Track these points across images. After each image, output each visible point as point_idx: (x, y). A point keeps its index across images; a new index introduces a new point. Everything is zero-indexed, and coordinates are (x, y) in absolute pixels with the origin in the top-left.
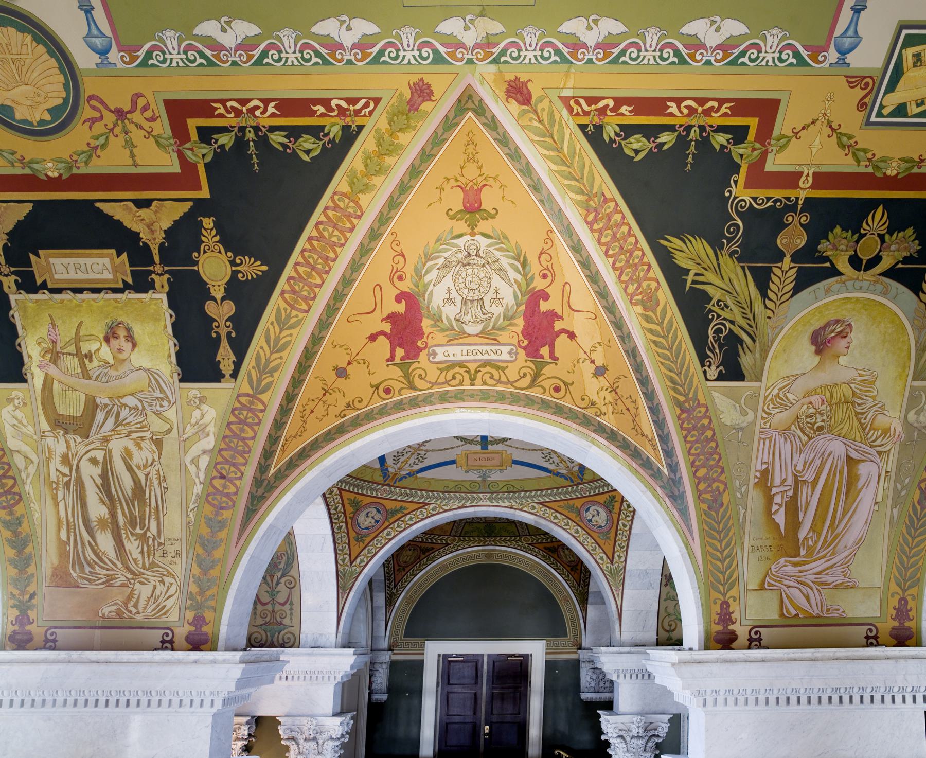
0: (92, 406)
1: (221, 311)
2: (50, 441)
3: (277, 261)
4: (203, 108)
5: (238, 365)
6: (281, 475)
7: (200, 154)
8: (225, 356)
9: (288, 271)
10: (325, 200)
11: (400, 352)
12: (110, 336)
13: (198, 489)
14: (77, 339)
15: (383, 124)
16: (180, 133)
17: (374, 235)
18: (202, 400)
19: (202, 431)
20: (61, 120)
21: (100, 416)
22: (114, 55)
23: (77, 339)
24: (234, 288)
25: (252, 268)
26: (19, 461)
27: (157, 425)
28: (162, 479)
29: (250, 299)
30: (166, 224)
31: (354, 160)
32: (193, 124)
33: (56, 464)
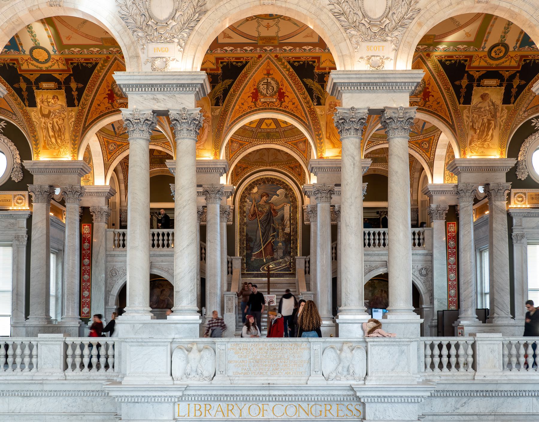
0: (50, 112)
1: (75, 93)
2: (41, 119)
3: (85, 84)
4: (72, 60)
5: (79, 104)
6: (88, 126)
7: (71, 67)
8: (76, 102)
9: (87, 86)
10: (93, 74)
11: (110, 101)
12: (53, 98)
13: (72, 129)
14: (47, 99)
15: (102, 62)
16: (67, 63)
17: (103, 80)
18: (72, 111)
19: (72, 117)
20: (47, 61)
21: (51, 114)
22: (57, 52)
23: (47, 99)
24: (77, 89)
25: (81, 85)
26: (35, 123)
27: (63, 116)
28: (64, 127)
29: (80, 91)
30: (64, 78)
31: (98, 67)
32: (69, 62)
33: (43, 124)
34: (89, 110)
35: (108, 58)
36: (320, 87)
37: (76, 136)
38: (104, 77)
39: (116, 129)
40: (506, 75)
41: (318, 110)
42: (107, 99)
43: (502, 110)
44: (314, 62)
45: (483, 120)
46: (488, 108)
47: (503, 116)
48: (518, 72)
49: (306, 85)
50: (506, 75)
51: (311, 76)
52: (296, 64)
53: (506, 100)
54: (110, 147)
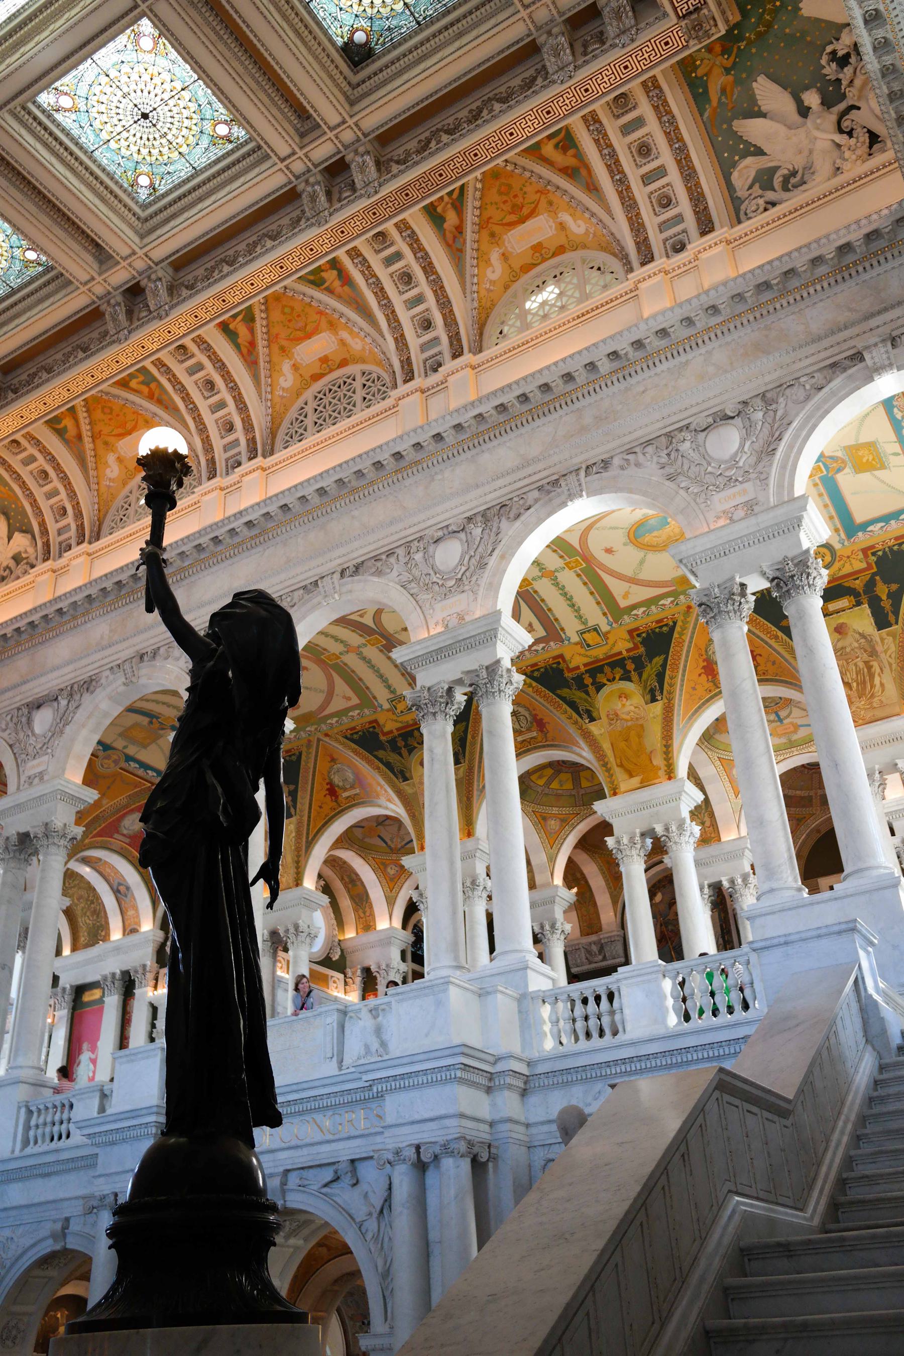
6: (313, 839)
17: (314, 772)
25: (292, 787)
34: (309, 817)
35: (309, 741)
36: (583, 695)
37: (298, 856)
38: (315, 768)
39: (389, 843)
40: (858, 584)
41: (594, 728)
42: (328, 797)
43: (882, 639)
44: (559, 663)
45: (856, 665)
46: (856, 645)
47: (888, 649)
48: (874, 574)
49: (563, 699)
50: (858, 584)
51: (566, 684)
52: (536, 674)
53: (882, 622)
54: (389, 870)
